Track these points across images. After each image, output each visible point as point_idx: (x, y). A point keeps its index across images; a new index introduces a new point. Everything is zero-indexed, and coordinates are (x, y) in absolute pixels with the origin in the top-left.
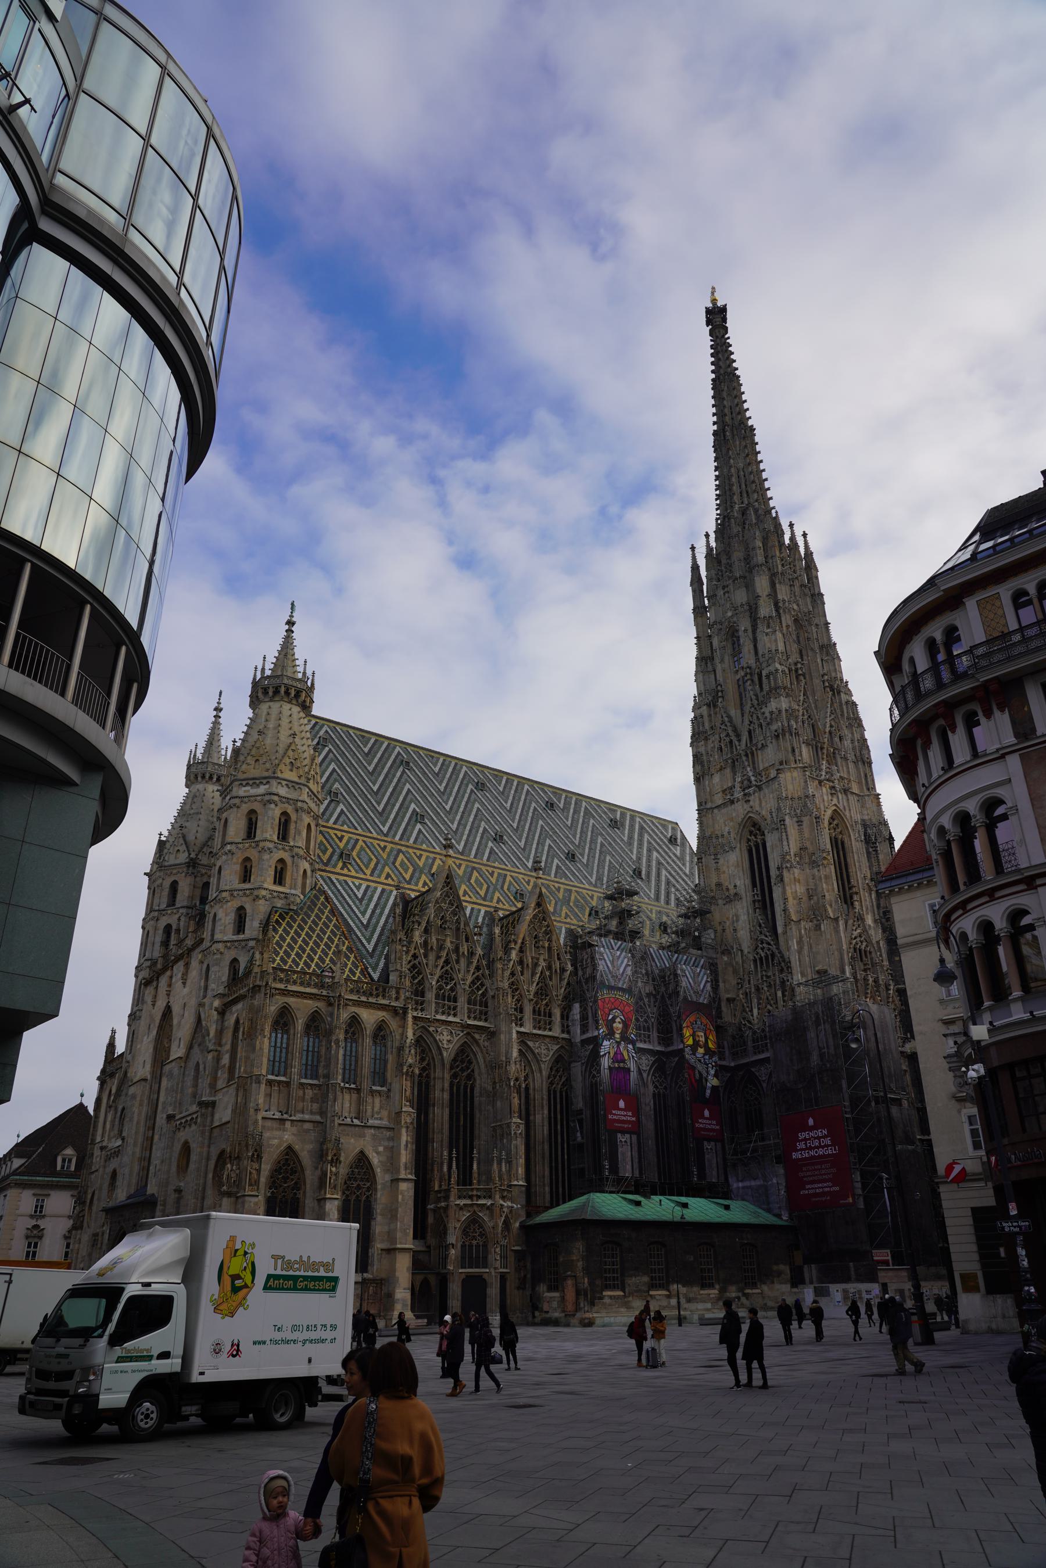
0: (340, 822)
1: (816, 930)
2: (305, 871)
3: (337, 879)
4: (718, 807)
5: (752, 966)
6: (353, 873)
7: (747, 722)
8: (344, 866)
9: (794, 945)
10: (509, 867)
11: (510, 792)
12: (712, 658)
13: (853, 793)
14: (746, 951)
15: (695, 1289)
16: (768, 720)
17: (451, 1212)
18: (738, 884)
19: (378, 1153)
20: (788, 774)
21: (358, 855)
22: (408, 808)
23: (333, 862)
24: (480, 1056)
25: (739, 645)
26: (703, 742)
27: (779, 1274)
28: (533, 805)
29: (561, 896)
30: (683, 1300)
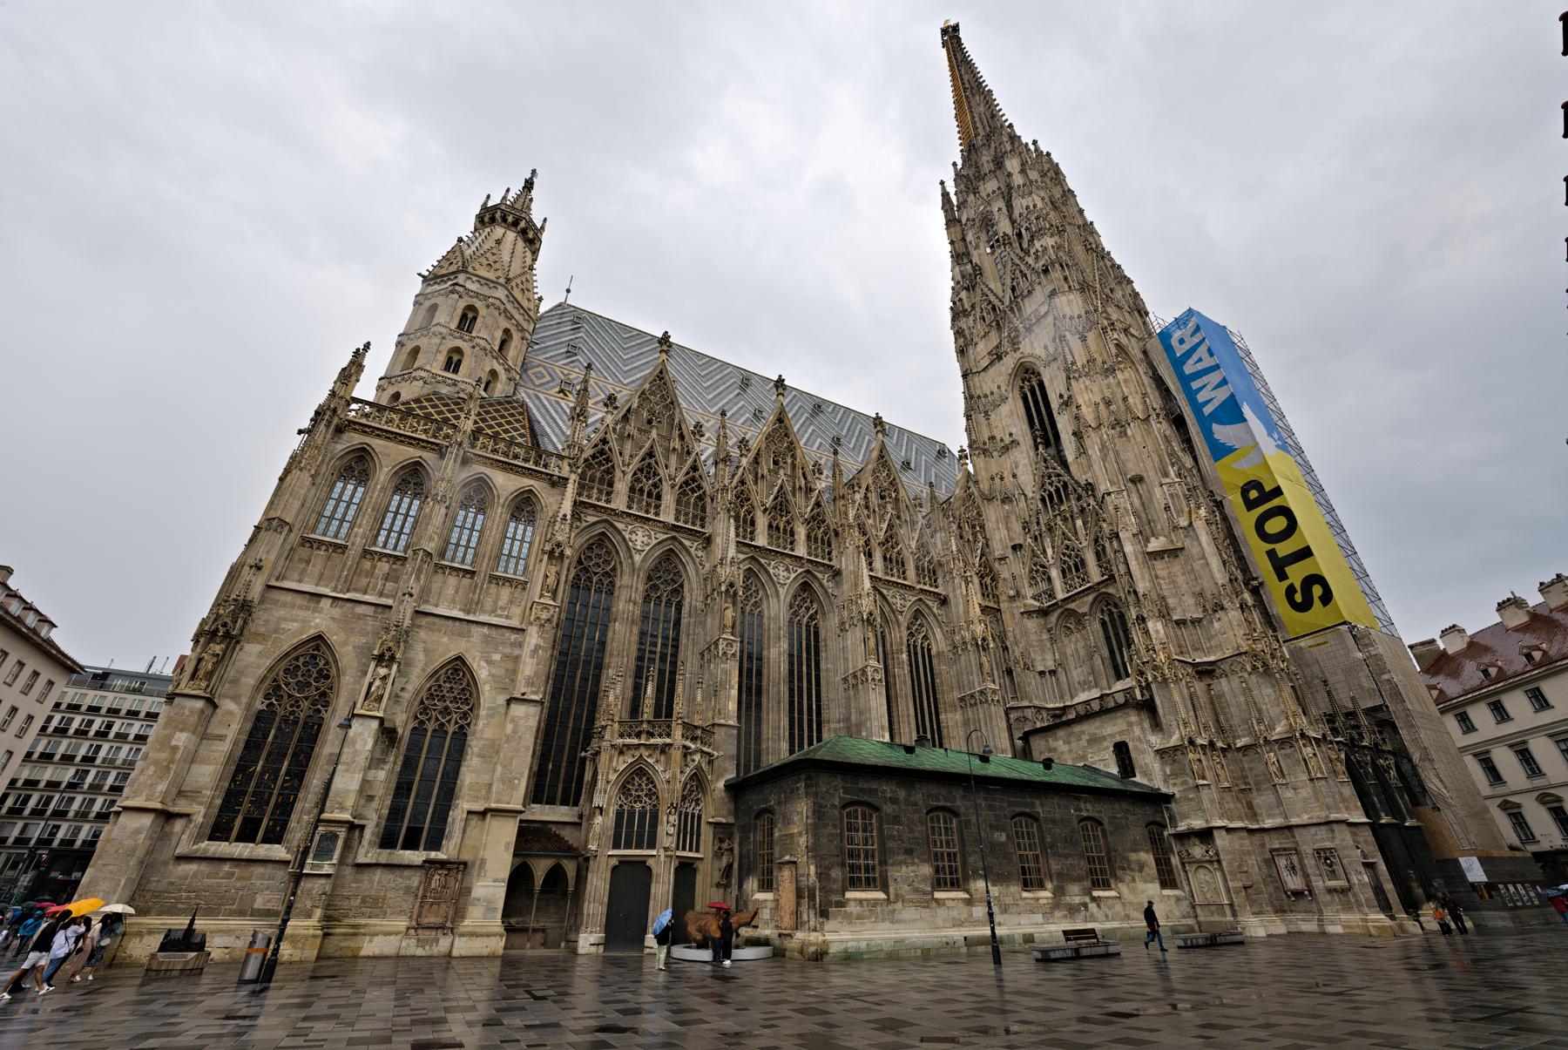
1: (1120, 437)
2: (493, 373)
4: (985, 369)
5: (1040, 506)
7: (1008, 281)
8: (561, 391)
9: (1094, 451)
12: (968, 254)
13: (1133, 336)
14: (1030, 495)
15: (1015, 889)
17: (604, 757)
18: (1014, 431)
19: (490, 662)
20: (1064, 298)
24: (691, 569)
27: (1142, 867)
30: (995, 909)
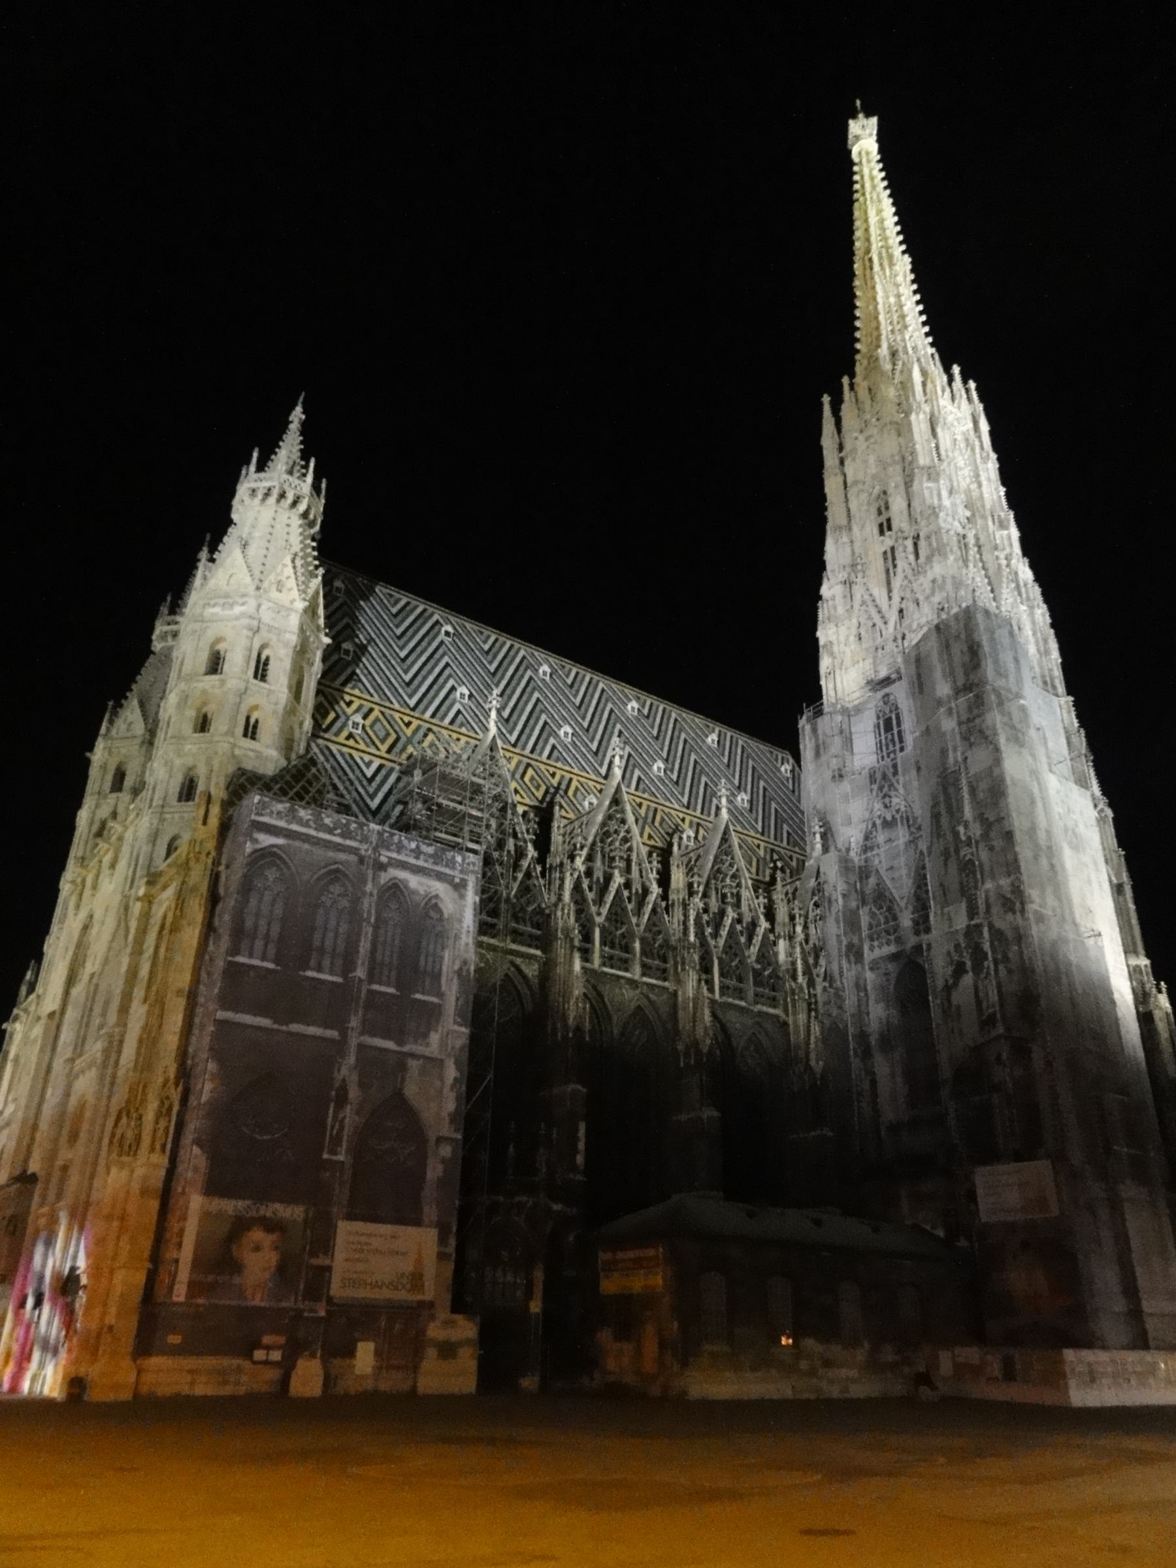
0: (350, 685)
3: (339, 751)
6: (362, 746)
7: (896, 598)
8: (350, 736)
10: (576, 771)
11: (579, 687)
12: (850, 529)
16: (928, 592)
21: (372, 726)
22: (446, 682)
23: (335, 729)
25: (887, 508)
26: (835, 629)
28: (610, 706)
29: (643, 812)
